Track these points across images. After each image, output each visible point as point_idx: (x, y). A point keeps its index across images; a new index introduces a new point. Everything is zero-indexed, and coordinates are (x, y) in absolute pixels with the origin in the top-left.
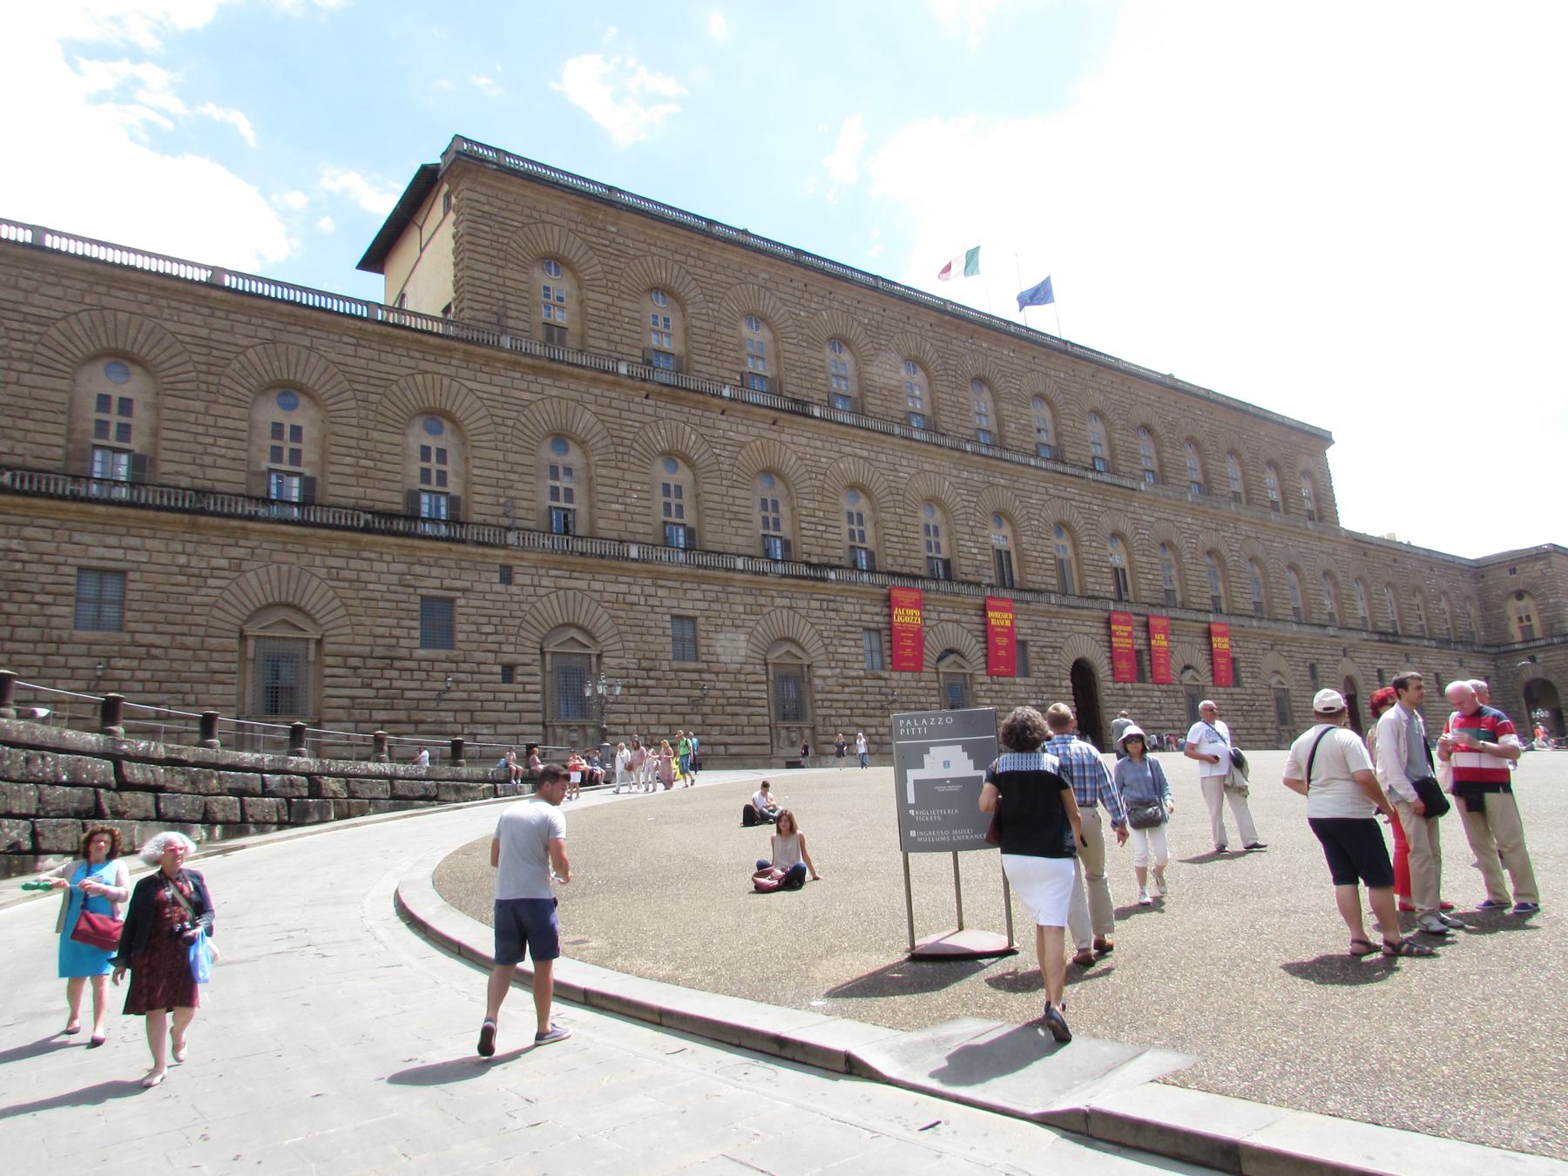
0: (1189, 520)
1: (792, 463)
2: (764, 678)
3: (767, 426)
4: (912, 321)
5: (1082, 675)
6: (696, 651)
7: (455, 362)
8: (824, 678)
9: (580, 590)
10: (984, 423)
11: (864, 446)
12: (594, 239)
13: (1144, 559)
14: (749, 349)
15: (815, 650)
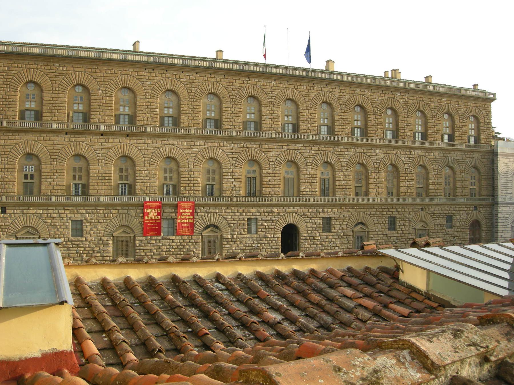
0: (378, 151)
1: (135, 152)
3: (124, 138)
6: (82, 233)
8: (141, 241)
9: (32, 214)
12: (48, 71)
13: (342, 173)
14: (122, 103)
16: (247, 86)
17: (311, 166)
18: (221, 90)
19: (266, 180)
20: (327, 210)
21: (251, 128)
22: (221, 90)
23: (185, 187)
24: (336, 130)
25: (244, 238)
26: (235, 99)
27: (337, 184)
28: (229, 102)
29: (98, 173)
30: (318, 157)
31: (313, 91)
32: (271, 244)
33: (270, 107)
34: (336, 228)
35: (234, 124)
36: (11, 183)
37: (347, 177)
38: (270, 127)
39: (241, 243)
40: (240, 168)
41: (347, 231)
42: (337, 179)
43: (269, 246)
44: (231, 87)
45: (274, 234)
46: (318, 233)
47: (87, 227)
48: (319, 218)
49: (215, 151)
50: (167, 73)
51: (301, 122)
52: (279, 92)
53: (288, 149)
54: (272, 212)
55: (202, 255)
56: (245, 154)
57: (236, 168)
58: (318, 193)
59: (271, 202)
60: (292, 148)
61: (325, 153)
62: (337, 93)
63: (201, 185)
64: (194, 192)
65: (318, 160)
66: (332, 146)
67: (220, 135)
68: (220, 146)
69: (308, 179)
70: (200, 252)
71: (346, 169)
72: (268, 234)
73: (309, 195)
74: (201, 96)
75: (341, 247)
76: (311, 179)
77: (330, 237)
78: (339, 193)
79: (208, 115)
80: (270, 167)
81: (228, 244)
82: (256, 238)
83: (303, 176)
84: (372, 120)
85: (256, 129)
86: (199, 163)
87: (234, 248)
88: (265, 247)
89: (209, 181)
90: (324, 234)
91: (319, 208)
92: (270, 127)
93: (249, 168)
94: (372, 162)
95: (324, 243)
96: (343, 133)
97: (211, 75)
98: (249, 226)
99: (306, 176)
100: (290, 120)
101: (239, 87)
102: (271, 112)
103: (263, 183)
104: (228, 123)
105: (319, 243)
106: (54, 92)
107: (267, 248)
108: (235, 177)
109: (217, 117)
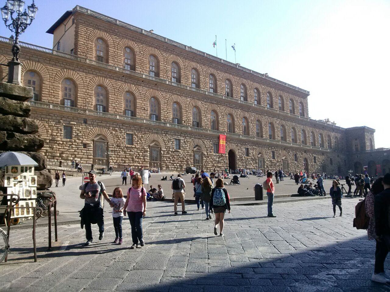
2: (149, 150)
4: (195, 58)
5: (232, 154)
7: (74, 66)
10: (212, 86)
11: (179, 92)
15: (162, 144)
23: (184, 121)
29: (141, 105)
32: (224, 160)
34: (251, 155)
36: (90, 103)
47: (135, 139)
50: (174, 51)
60: (231, 106)
64: (189, 124)
76: (239, 125)
90: (246, 157)
102: (221, 85)
106: (115, 48)
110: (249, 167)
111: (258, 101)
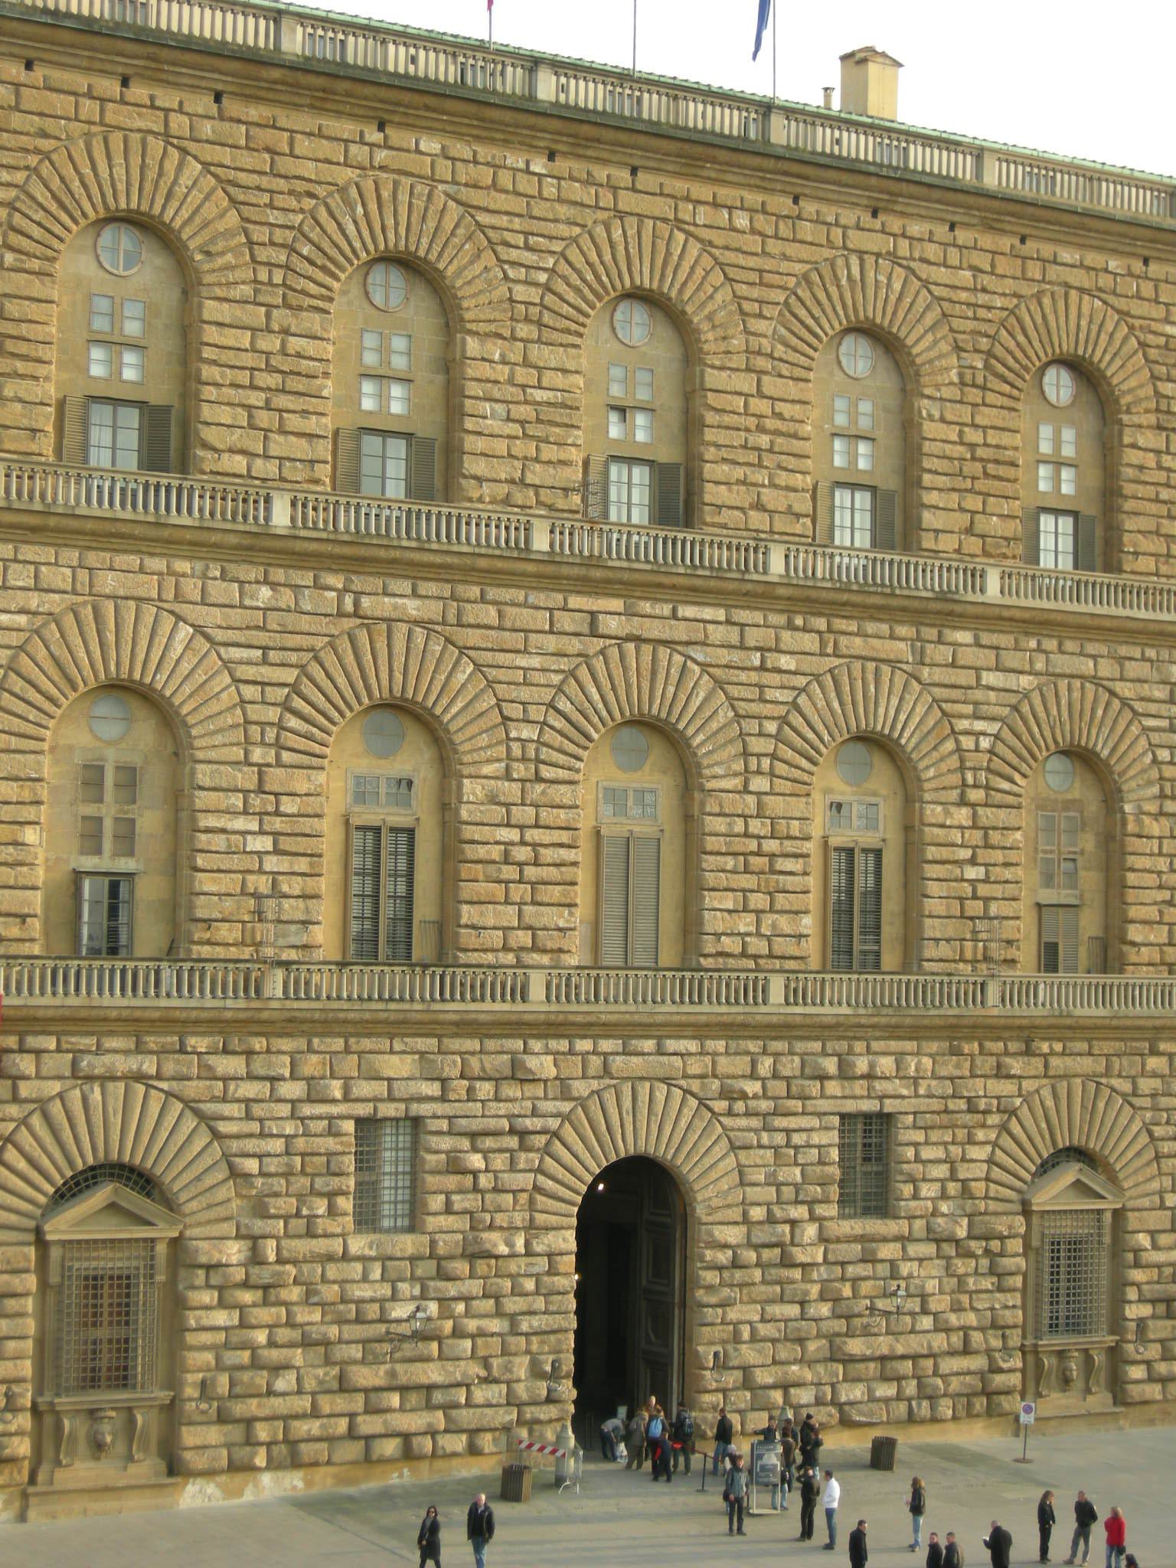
13: (962, 815)
16: (369, 186)
17: (774, 756)
18: (196, 197)
19: (481, 852)
20: (872, 1066)
21: (383, 478)
22: (196, 197)
24: (928, 518)
25: (330, 1258)
26: (287, 267)
27: (933, 888)
28: (247, 290)
30: (817, 703)
31: (792, 249)
32: (512, 1305)
33: (514, 338)
34: (928, 1190)
35: (279, 445)
37: (995, 837)
38: (512, 482)
39: (310, 1297)
40: (314, 760)
41: (993, 1206)
42: (932, 852)
43: (499, 1313)
44: (265, 182)
45: (532, 1228)
46: (813, 1218)
48: (820, 1115)
49: (144, 633)
51: (710, 453)
52: (575, 240)
53: (629, 638)
54: (518, 1074)
55: (39, 1391)
56: (350, 659)
57: (286, 756)
58: (811, 948)
59: (520, 1007)
61: (857, 673)
62: (941, 274)
63: (40, 875)
65: (815, 719)
66: (902, 630)
67: (185, 520)
68: (178, 597)
69: (753, 845)
70: (27, 1368)
71: (988, 787)
72: (491, 1227)
73: (755, 957)
74: (57, 229)
75: (953, 1319)
76: (770, 846)
77: (888, 1251)
78: (944, 950)
79: (97, 370)
80: (509, 757)
81: (222, 1304)
82: (413, 1259)
83: (718, 824)
84: (1150, 460)
85: (419, 488)
86: (33, 714)
87: (261, 1337)
88: (472, 1325)
89: (98, 851)
91: (816, 1046)
92: (512, 482)
93: (365, 765)
94: (1143, 742)
95: (847, 1291)
96: (973, 545)
97: (125, 82)
98: (367, 1177)
99: (739, 826)
100: (641, 436)
101: (321, 191)
102: (522, 375)
103: (465, 870)
104: (234, 438)
105: (815, 1290)
107: (481, 1333)
108: (278, 824)
109: (160, 394)
110: (883, 1345)
111: (1090, 509)
